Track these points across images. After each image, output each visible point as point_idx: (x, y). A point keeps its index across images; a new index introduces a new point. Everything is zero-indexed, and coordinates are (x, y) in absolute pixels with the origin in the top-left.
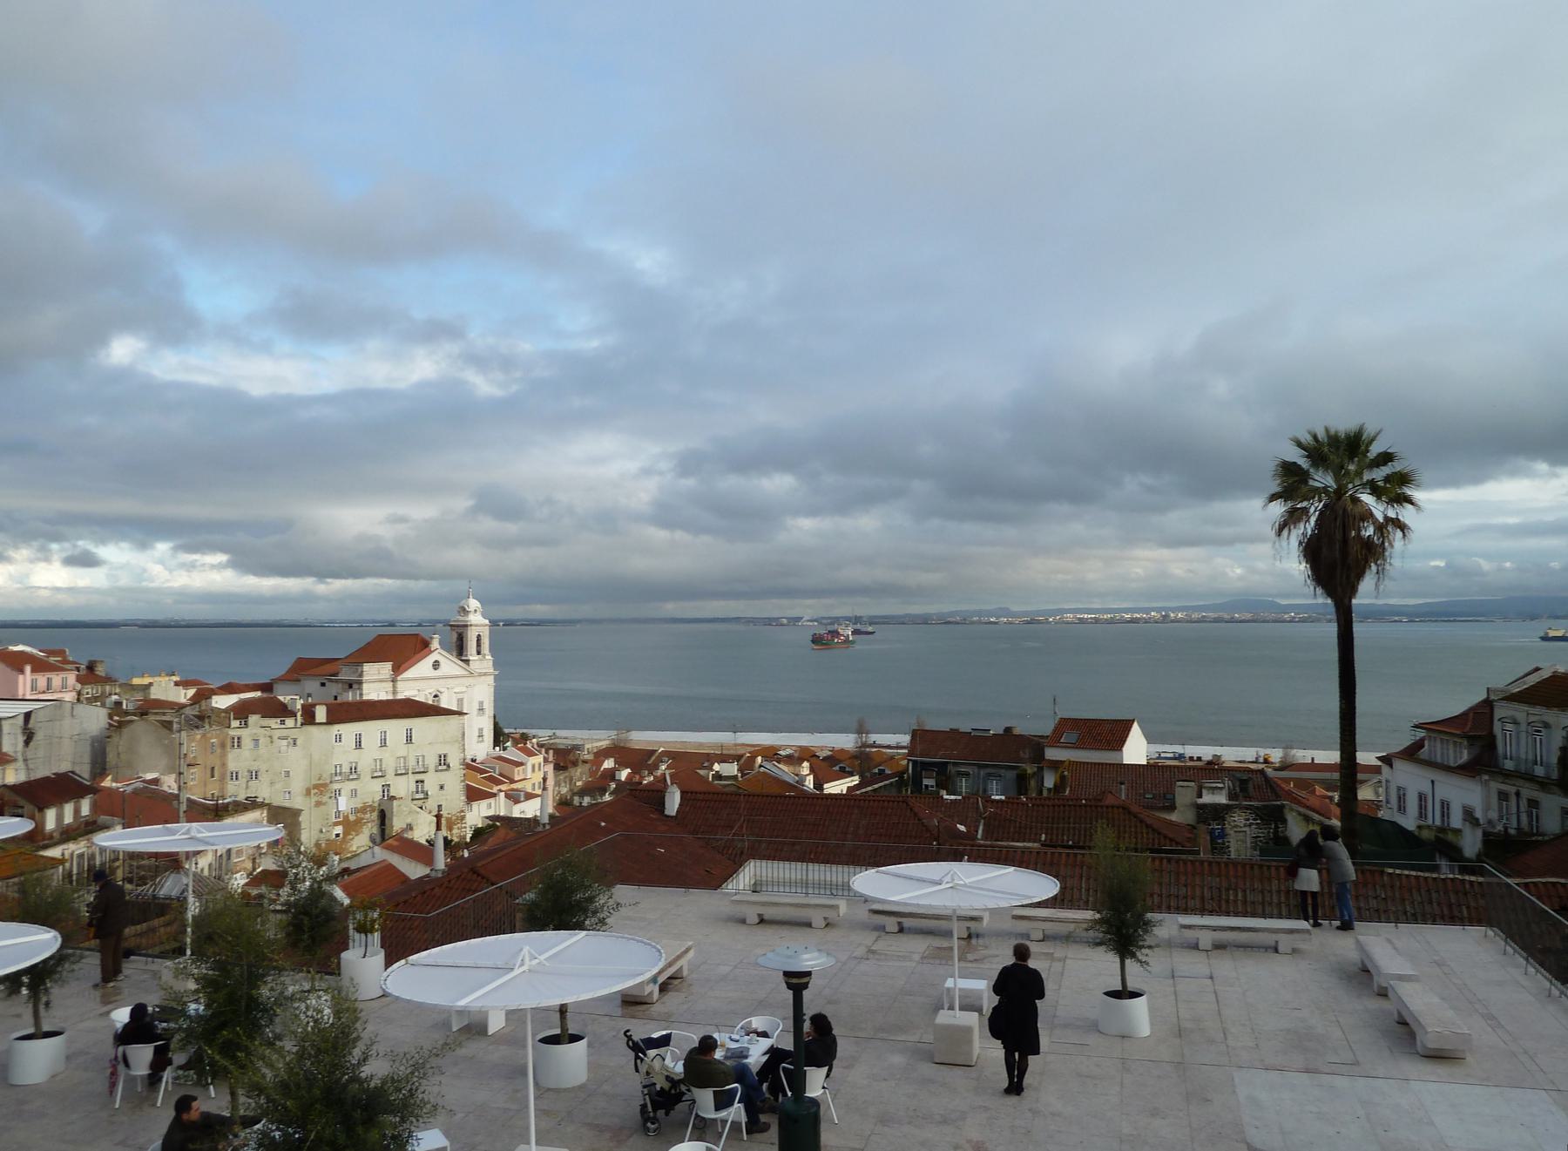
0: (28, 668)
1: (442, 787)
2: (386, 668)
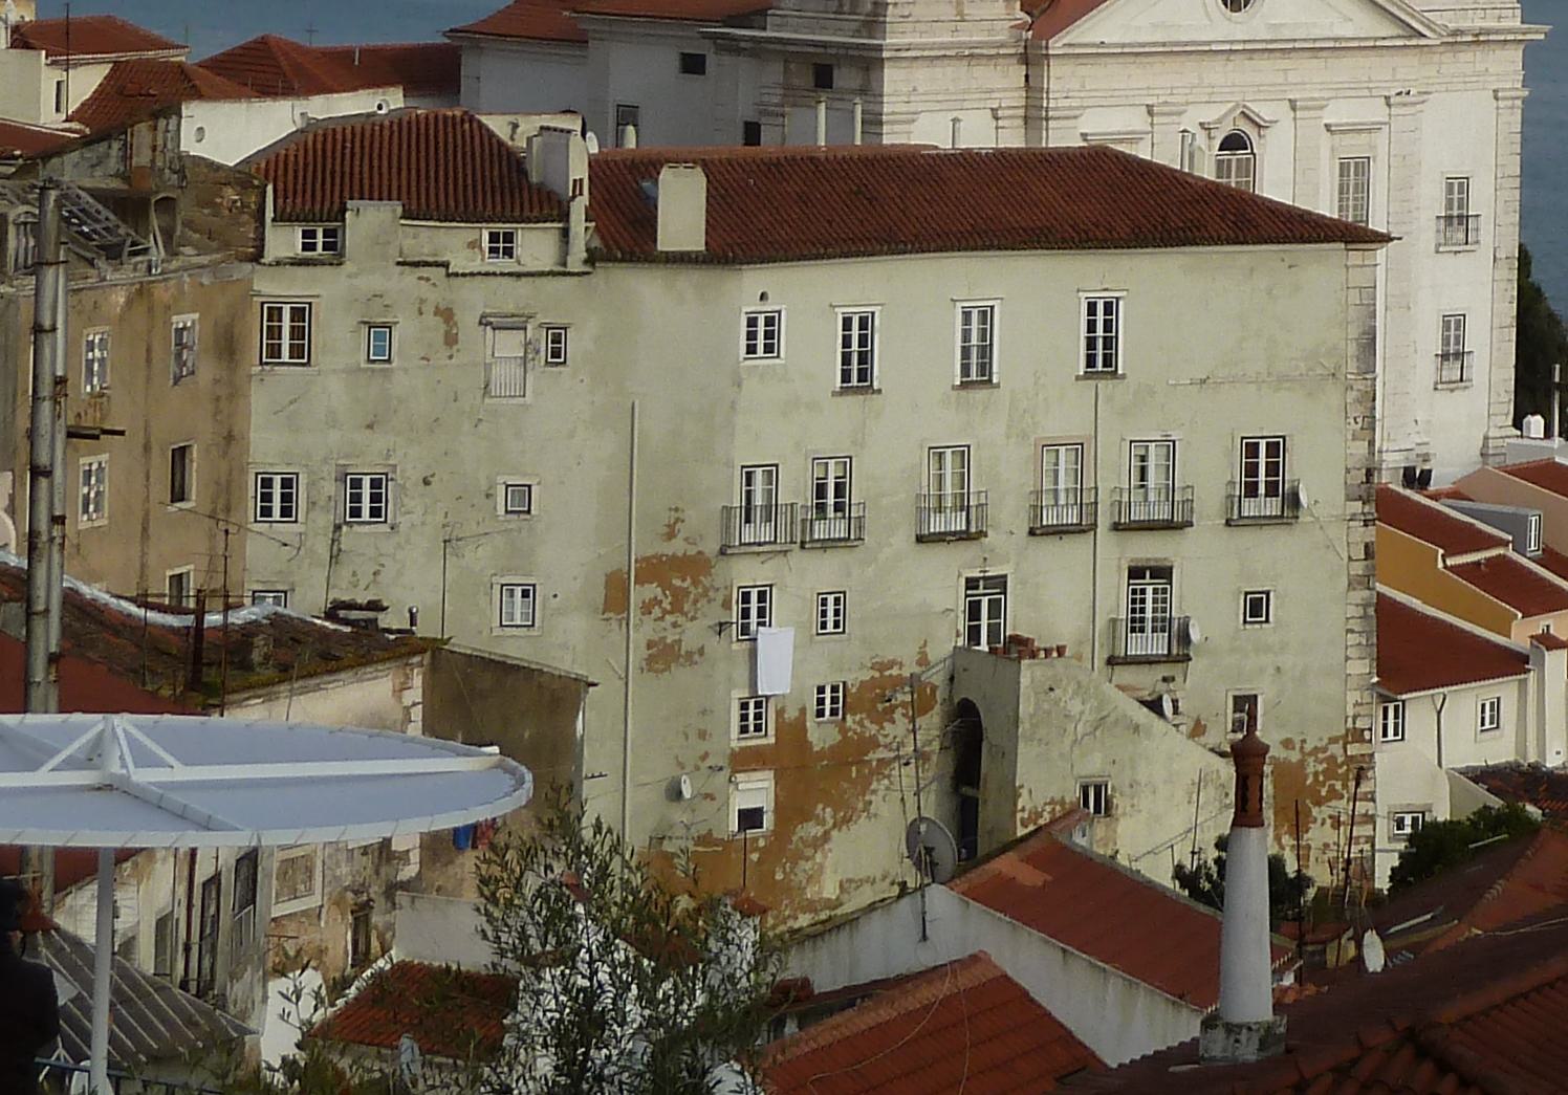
1: (1256, 607)
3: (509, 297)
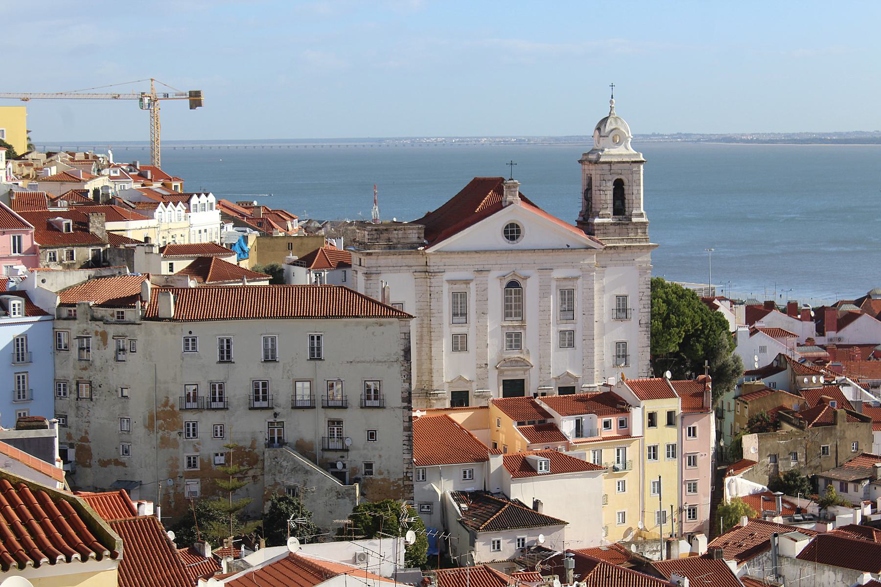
1: (372, 435)
3: (122, 329)
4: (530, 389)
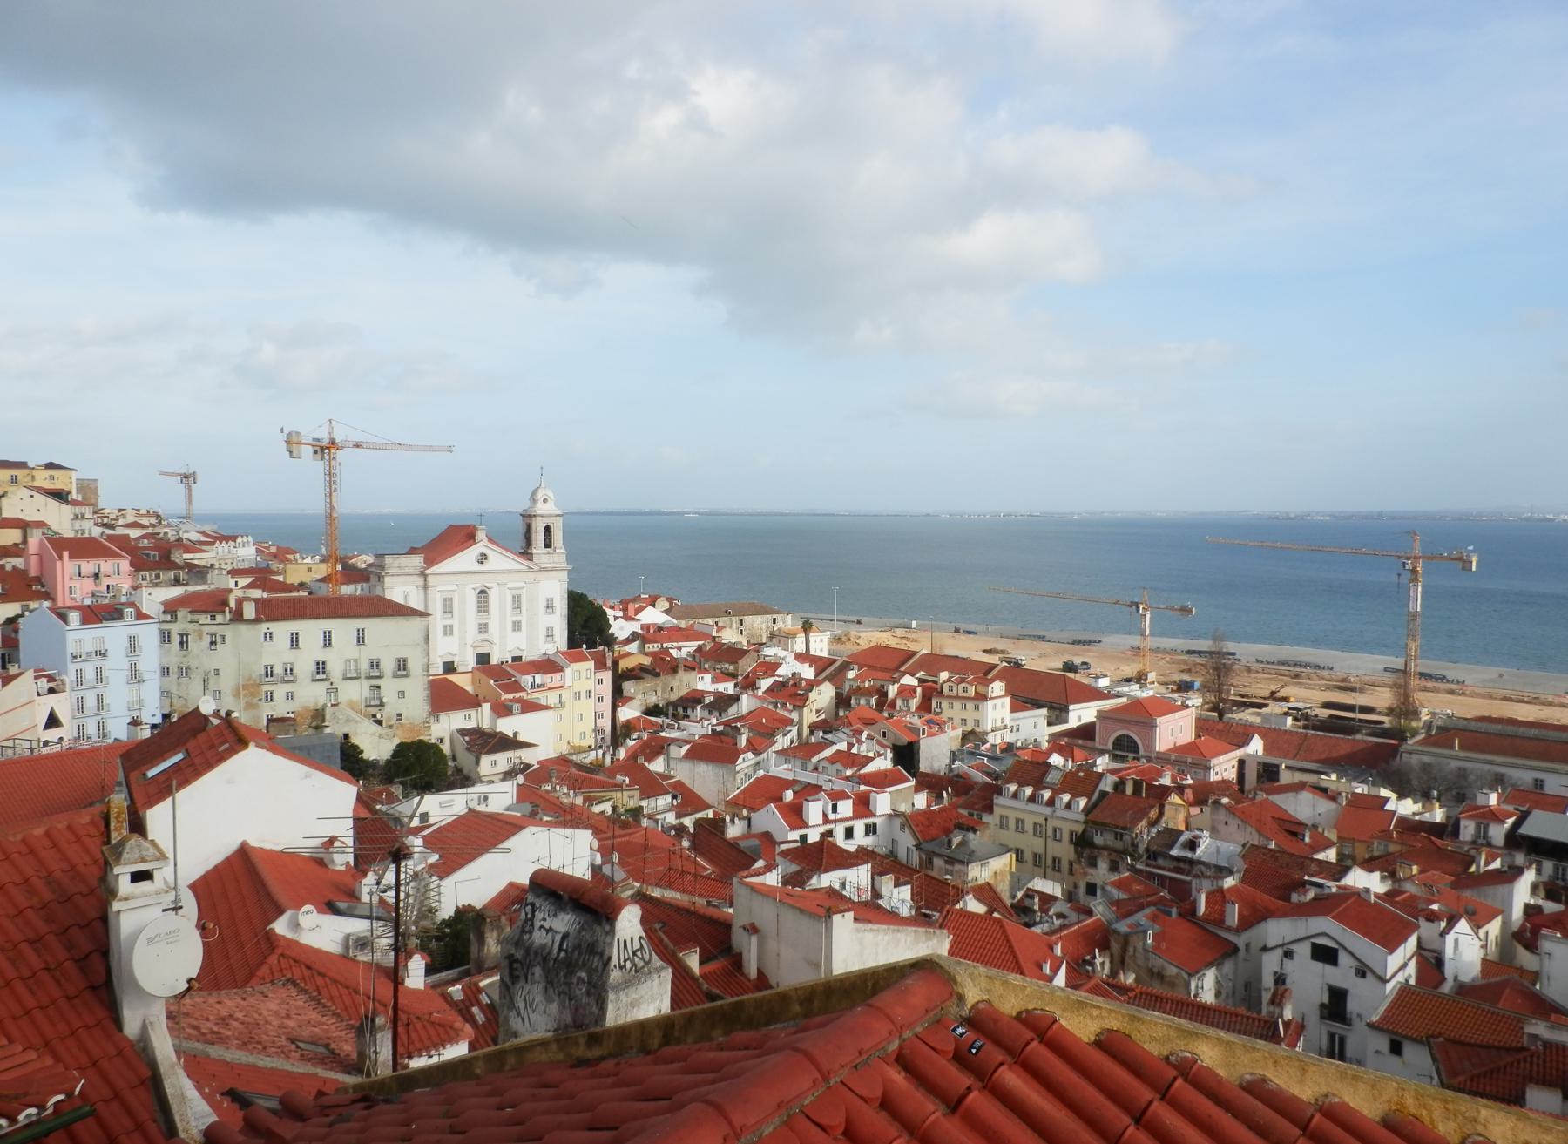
0: (66, 554)
1: (402, 694)
2: (417, 561)
3: (213, 629)
4: (494, 661)
